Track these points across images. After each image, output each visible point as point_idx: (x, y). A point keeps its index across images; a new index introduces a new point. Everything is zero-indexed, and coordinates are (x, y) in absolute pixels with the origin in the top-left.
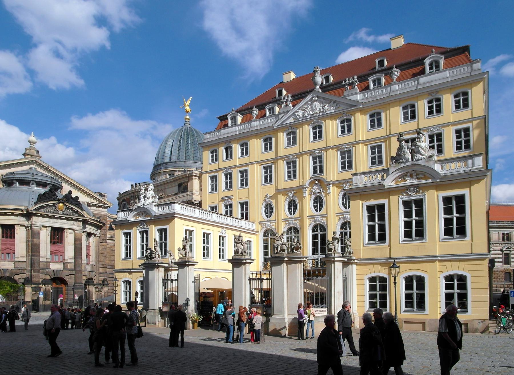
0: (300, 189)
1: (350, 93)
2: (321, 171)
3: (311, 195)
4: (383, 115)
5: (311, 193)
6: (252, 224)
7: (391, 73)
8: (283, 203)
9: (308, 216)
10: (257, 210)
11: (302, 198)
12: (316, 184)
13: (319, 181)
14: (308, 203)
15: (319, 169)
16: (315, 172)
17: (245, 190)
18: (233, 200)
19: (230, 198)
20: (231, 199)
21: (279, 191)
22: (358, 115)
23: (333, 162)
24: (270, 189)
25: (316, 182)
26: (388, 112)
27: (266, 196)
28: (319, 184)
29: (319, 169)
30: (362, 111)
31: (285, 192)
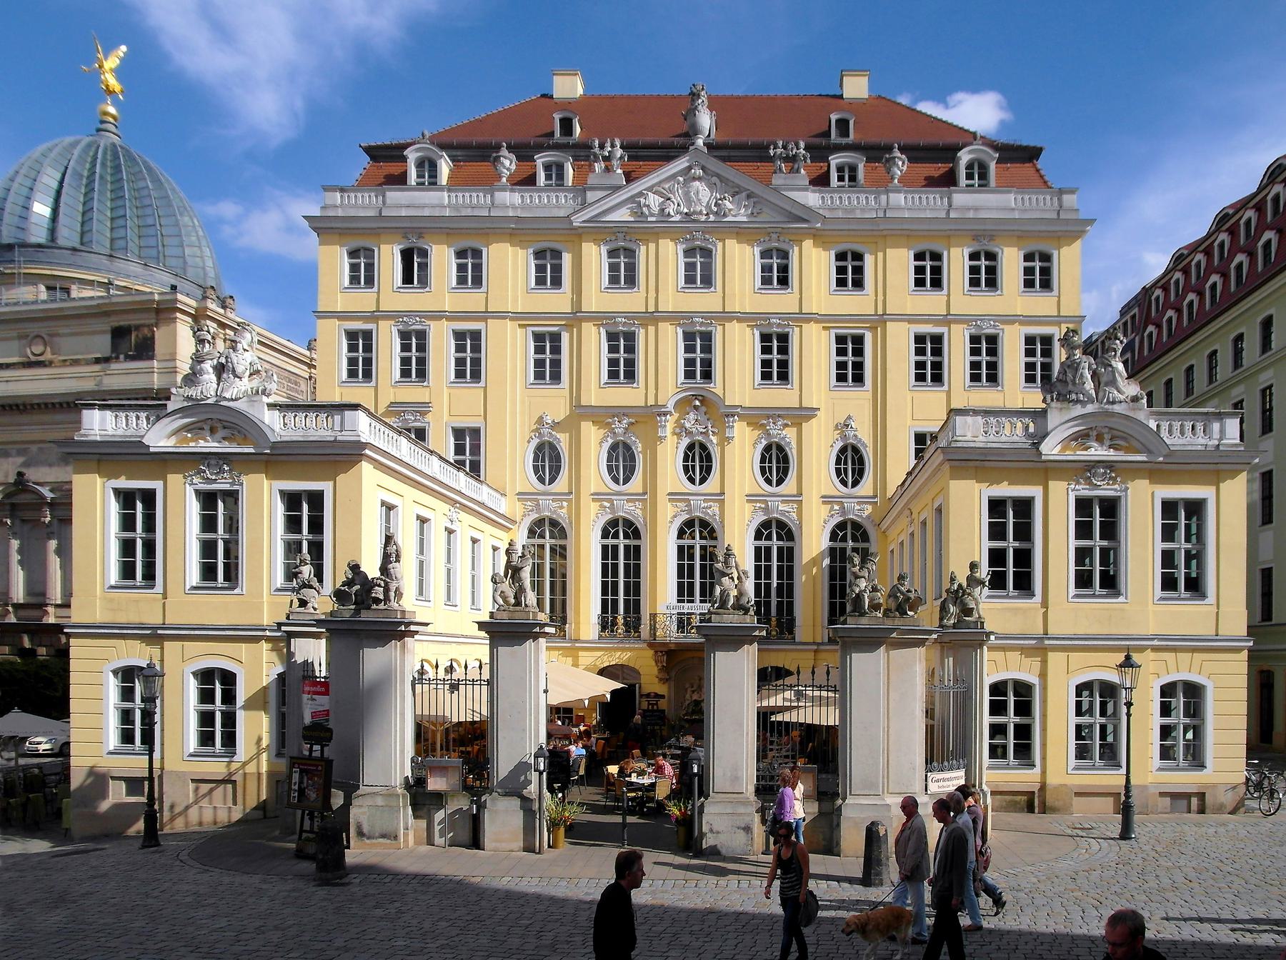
0: (649, 416)
1: (788, 182)
2: (707, 375)
3: (679, 435)
4: (869, 261)
5: (681, 430)
6: (498, 496)
7: (888, 160)
8: (594, 445)
9: (670, 494)
10: (510, 456)
11: (654, 441)
12: (696, 408)
13: (704, 401)
14: (671, 454)
15: (700, 365)
16: (689, 375)
17: (470, 394)
18: (429, 418)
19: (422, 408)
20: (423, 414)
21: (581, 412)
22: (808, 244)
23: (738, 354)
24: (555, 402)
25: (697, 403)
26: (880, 255)
27: (540, 420)
28: (704, 409)
29: (700, 365)
30: (820, 238)
31: (603, 416)
